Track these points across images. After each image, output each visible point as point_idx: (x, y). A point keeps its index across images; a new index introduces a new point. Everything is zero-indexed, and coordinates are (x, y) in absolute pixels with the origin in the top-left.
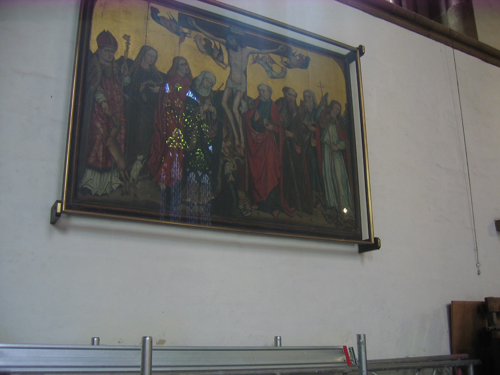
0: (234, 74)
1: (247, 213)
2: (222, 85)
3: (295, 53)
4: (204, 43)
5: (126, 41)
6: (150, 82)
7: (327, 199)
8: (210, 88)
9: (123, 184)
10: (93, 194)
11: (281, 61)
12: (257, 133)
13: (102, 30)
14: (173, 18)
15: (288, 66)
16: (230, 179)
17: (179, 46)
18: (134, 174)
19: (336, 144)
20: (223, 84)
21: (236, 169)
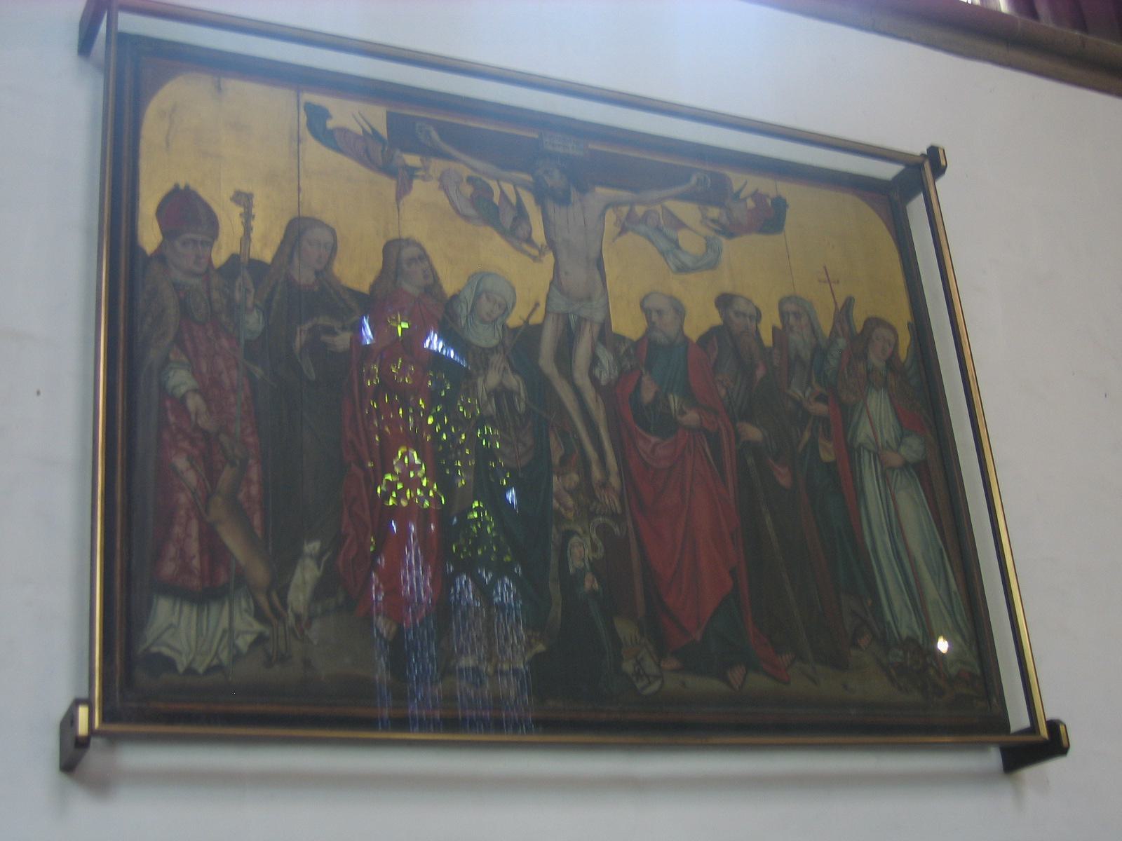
0: (566, 273)
1: (650, 683)
2: (534, 310)
3: (740, 191)
4: (468, 190)
5: (241, 210)
6: (323, 320)
7: (889, 617)
8: (500, 320)
9: (267, 632)
10: (181, 669)
12: (654, 440)
13: (168, 187)
14: (373, 130)
16: (588, 585)
18: (299, 597)
19: (894, 445)
20: (537, 305)
21: (600, 554)
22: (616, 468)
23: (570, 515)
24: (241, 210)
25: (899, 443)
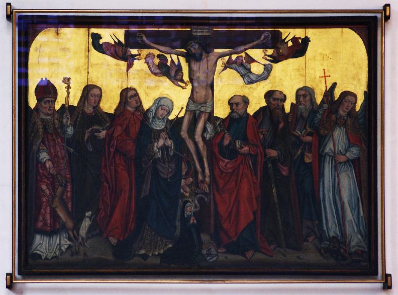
0: (197, 92)
1: (213, 257)
3: (286, 38)
4: (157, 61)
5: (66, 85)
10: (43, 258)
11: (263, 55)
12: (227, 161)
14: (119, 40)
15: (276, 59)
16: (191, 221)
17: (127, 75)
18: (83, 232)
19: (344, 153)
20: (182, 108)
21: (198, 209)
22: (209, 174)
23: (187, 194)
24: (66, 85)
25: (347, 150)
